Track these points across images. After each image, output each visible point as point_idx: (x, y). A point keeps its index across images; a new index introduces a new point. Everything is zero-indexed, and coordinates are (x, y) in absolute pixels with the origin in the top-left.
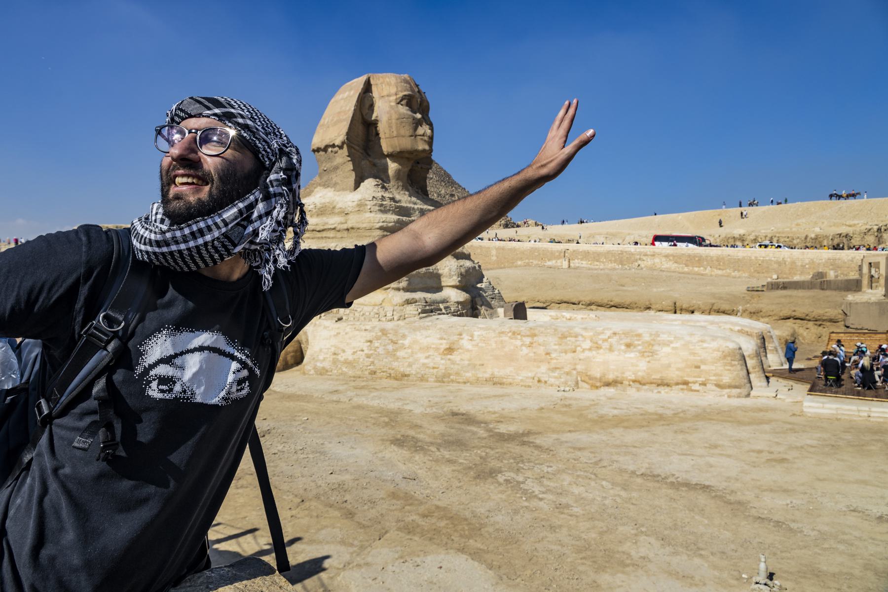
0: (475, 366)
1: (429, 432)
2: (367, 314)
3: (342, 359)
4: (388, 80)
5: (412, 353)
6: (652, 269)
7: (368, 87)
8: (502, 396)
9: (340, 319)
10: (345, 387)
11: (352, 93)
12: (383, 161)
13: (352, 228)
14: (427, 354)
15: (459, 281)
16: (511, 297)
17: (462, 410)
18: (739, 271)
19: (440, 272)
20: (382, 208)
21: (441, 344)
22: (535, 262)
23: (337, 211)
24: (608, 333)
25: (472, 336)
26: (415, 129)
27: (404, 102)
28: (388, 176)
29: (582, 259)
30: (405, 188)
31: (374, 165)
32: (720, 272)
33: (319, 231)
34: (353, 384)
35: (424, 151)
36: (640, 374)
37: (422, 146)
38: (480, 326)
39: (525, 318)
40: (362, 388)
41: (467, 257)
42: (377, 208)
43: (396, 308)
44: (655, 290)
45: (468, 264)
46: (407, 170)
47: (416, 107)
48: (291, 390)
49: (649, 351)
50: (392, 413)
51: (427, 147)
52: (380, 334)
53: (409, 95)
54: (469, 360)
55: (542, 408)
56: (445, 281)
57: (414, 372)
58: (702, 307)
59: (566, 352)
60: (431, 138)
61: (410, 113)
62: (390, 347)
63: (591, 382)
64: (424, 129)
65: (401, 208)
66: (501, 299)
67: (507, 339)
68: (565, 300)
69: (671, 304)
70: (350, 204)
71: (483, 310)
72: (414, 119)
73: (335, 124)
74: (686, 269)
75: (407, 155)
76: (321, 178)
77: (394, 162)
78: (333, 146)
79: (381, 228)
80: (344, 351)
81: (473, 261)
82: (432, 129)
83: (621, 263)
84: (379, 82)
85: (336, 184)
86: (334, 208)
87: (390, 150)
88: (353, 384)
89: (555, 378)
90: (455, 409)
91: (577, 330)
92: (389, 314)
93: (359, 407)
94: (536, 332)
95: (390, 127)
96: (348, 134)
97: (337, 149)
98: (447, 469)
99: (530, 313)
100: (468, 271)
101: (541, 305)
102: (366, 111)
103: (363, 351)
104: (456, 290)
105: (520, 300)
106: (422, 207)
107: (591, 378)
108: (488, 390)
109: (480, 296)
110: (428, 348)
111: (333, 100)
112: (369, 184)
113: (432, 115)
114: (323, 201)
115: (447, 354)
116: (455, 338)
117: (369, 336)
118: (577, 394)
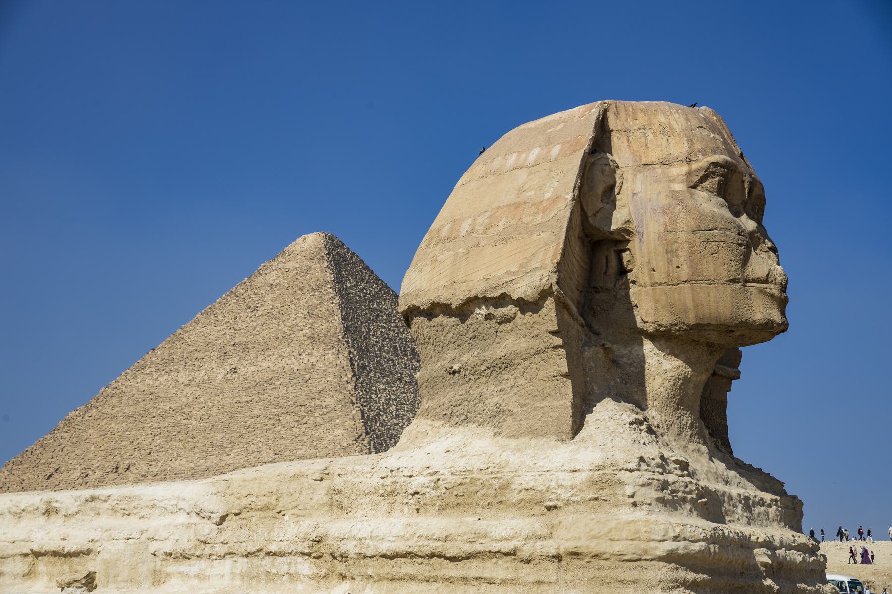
13: (575, 555)
23: (514, 497)
33: (454, 559)
79: (670, 558)
86: (505, 487)
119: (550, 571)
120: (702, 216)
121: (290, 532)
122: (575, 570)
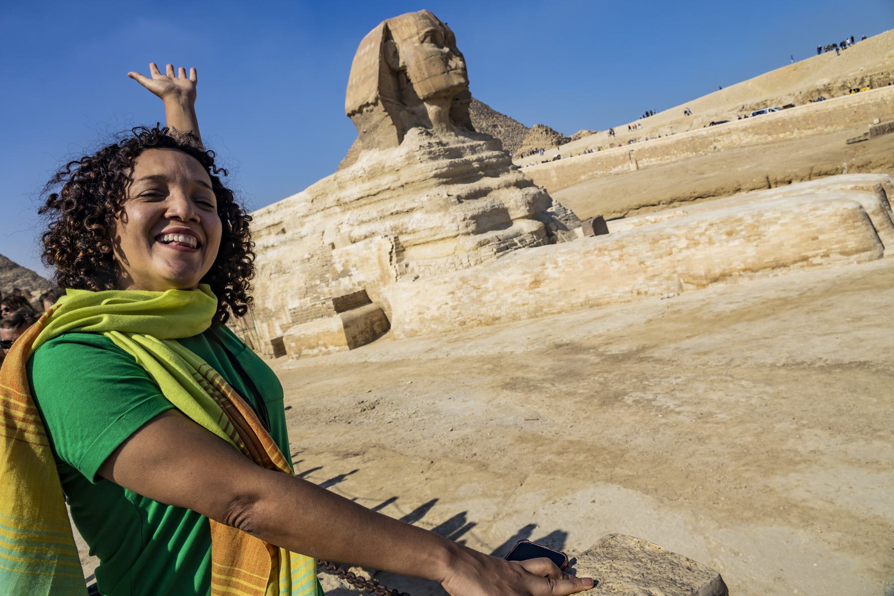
0: (566, 293)
1: (537, 369)
2: (442, 266)
3: (428, 317)
4: (406, 21)
5: (498, 294)
6: (729, 148)
7: (387, 35)
8: (603, 317)
9: (417, 278)
10: (439, 343)
11: (373, 44)
12: (421, 107)
14: (513, 292)
15: (528, 211)
16: (585, 213)
17: (566, 340)
18: (832, 125)
19: (506, 206)
20: (432, 156)
21: (526, 279)
22: (600, 173)
23: (387, 170)
24: (704, 226)
25: (556, 263)
26: (446, 64)
27: (428, 39)
28: (430, 121)
29: (650, 157)
30: (449, 129)
31: (413, 113)
32: (810, 132)
34: (446, 339)
35: (460, 85)
36: (750, 261)
37: (457, 80)
38: (562, 251)
39: (606, 231)
40: (456, 340)
41: (530, 184)
42: (427, 156)
43: (470, 253)
44: (740, 169)
45: (532, 190)
46: (447, 109)
47: (441, 41)
48: (387, 358)
49: (755, 233)
50: (493, 358)
51: (462, 80)
52: (460, 283)
53: (431, 31)
54: (559, 288)
55: (650, 321)
56: (513, 214)
57: (504, 314)
58: (800, 174)
59: (661, 257)
60: (464, 69)
61: (436, 49)
62: (474, 294)
63: (695, 282)
64: (455, 62)
65: (450, 150)
66: (576, 218)
67: (594, 257)
68: (643, 204)
69: (763, 179)
70: (399, 159)
71: (559, 234)
72: (442, 54)
73: (364, 82)
74: (770, 139)
75: (444, 94)
76: (363, 142)
77: (432, 104)
78: (368, 105)
79: (436, 176)
80: (428, 309)
81: (537, 187)
82: (463, 60)
83: (695, 149)
84: (397, 26)
85: (379, 143)
86: (383, 167)
87: (426, 93)
88: (446, 339)
89: (655, 286)
90: (558, 341)
91: (669, 230)
92: (465, 261)
93: (458, 360)
94: (624, 243)
95: (420, 69)
96: (379, 88)
97: (371, 107)
98: (568, 403)
99: (610, 225)
100: (534, 197)
101: (619, 215)
102: (391, 60)
103: (447, 304)
104: (526, 220)
105: (595, 215)
106: (471, 144)
107: (694, 277)
108: (586, 314)
109: (553, 220)
110: (513, 286)
111: (355, 58)
112: (413, 135)
113: (459, 46)
114: (371, 163)
115: (535, 288)
116: (539, 269)
117: (450, 287)
118: (684, 297)
119: (401, 191)
120: (427, 53)
121: (330, 200)
122: (408, 188)
